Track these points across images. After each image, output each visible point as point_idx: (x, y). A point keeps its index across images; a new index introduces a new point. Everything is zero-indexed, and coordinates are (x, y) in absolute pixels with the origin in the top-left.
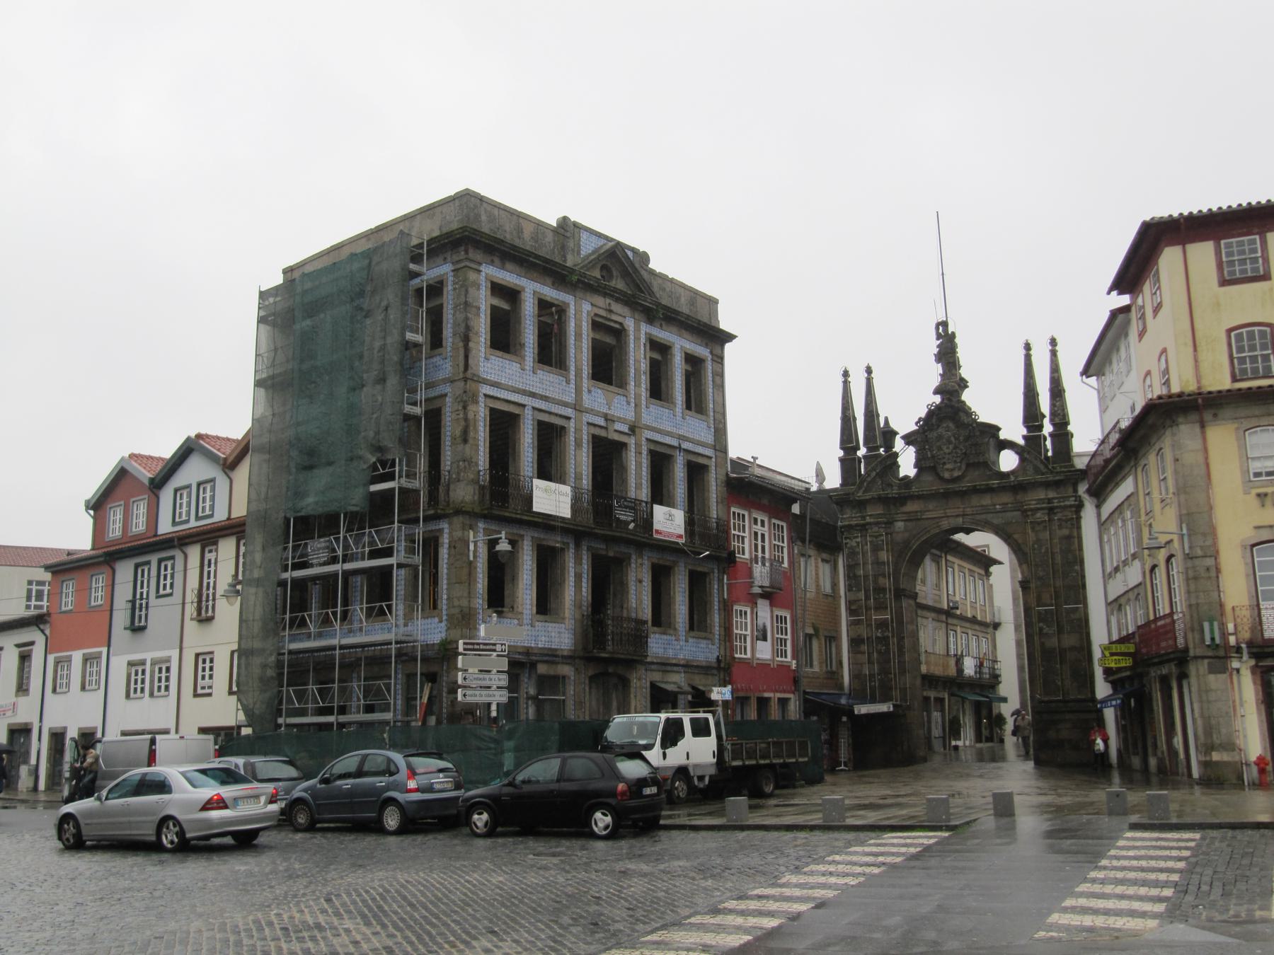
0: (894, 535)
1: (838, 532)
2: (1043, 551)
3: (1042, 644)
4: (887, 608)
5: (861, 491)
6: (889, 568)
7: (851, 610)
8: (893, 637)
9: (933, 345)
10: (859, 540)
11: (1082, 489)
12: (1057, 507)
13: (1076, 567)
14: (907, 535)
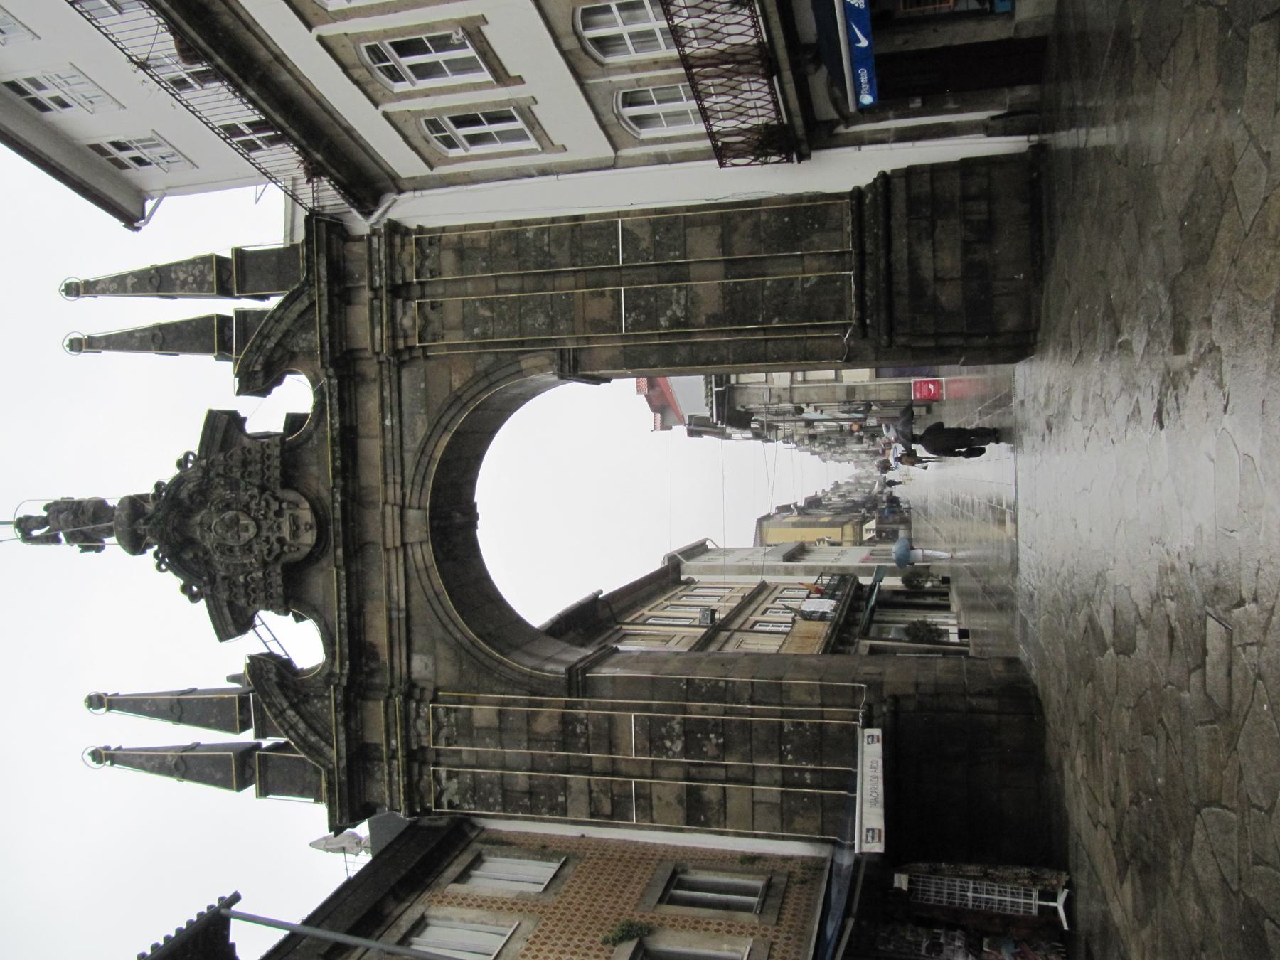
0: (441, 682)
1: (425, 821)
2: (487, 313)
3: (713, 319)
4: (610, 719)
5: (326, 749)
6: (515, 703)
7: (612, 817)
8: (684, 710)
9: (66, 552)
10: (443, 771)
11: (360, 225)
12: (391, 277)
13: (530, 235)
14: (441, 650)
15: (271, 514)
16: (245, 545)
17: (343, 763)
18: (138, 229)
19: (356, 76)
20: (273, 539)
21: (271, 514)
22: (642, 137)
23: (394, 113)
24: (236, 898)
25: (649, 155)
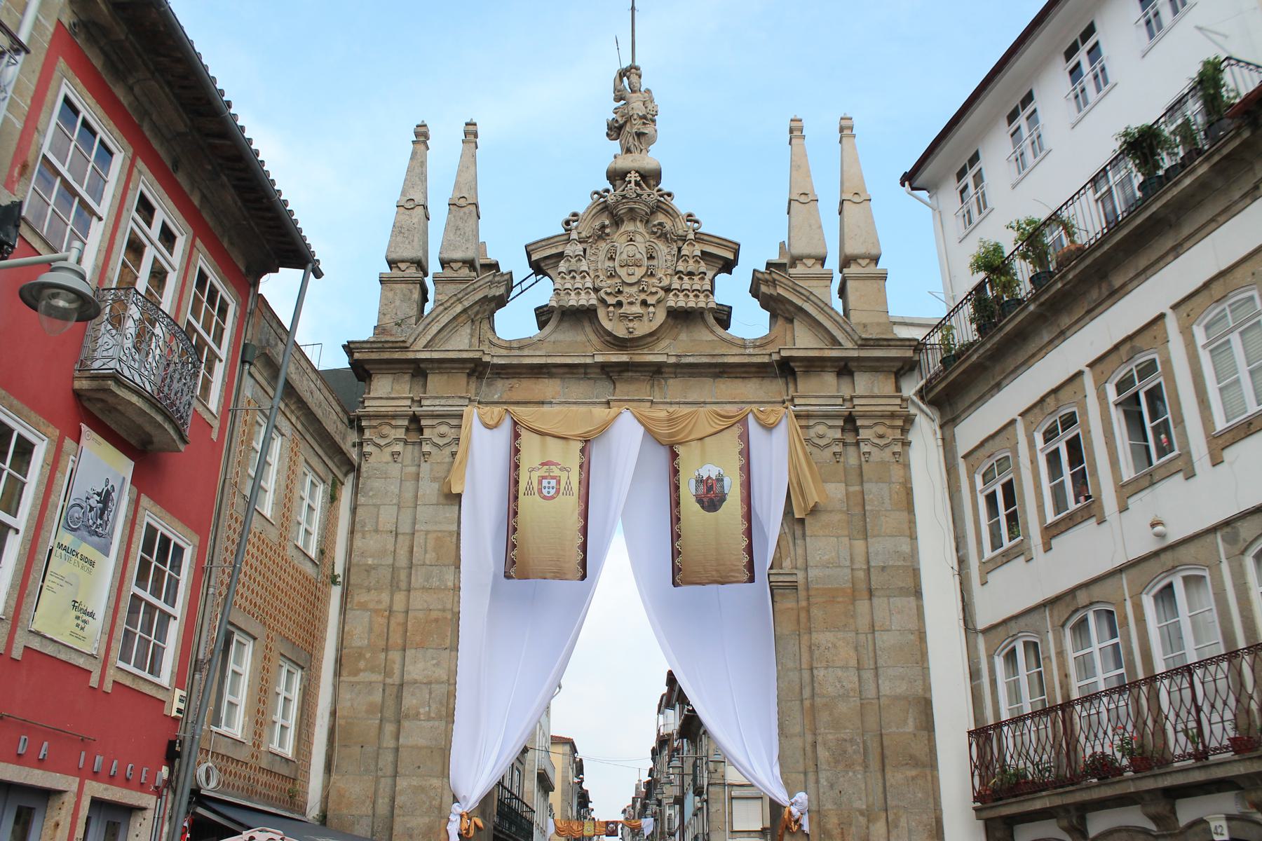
11: (910, 388)
15: (643, 296)
16: (615, 271)
17: (411, 356)
18: (903, 185)
19: (1048, 400)
20: (620, 298)
21: (643, 296)
22: (996, 658)
23: (1016, 430)
24: (318, 274)
25: (979, 663)
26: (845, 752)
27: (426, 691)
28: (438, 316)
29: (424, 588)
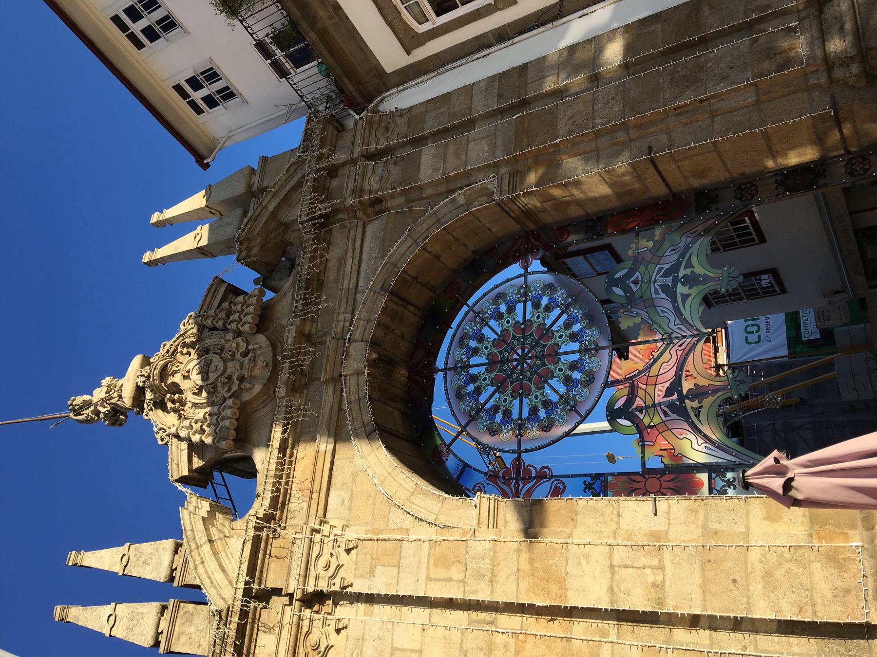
15: (238, 356)
26: (684, 76)
27: (623, 573)
28: (206, 572)
29: (491, 581)
